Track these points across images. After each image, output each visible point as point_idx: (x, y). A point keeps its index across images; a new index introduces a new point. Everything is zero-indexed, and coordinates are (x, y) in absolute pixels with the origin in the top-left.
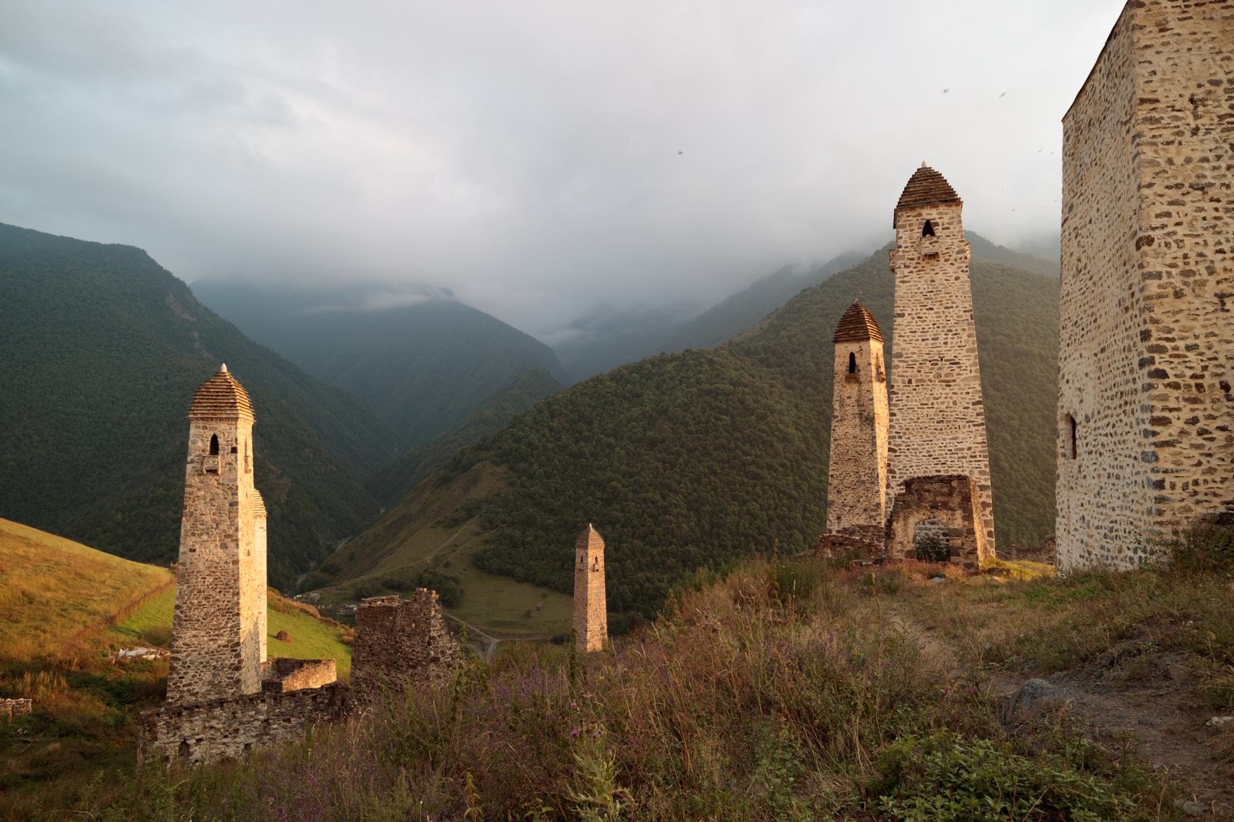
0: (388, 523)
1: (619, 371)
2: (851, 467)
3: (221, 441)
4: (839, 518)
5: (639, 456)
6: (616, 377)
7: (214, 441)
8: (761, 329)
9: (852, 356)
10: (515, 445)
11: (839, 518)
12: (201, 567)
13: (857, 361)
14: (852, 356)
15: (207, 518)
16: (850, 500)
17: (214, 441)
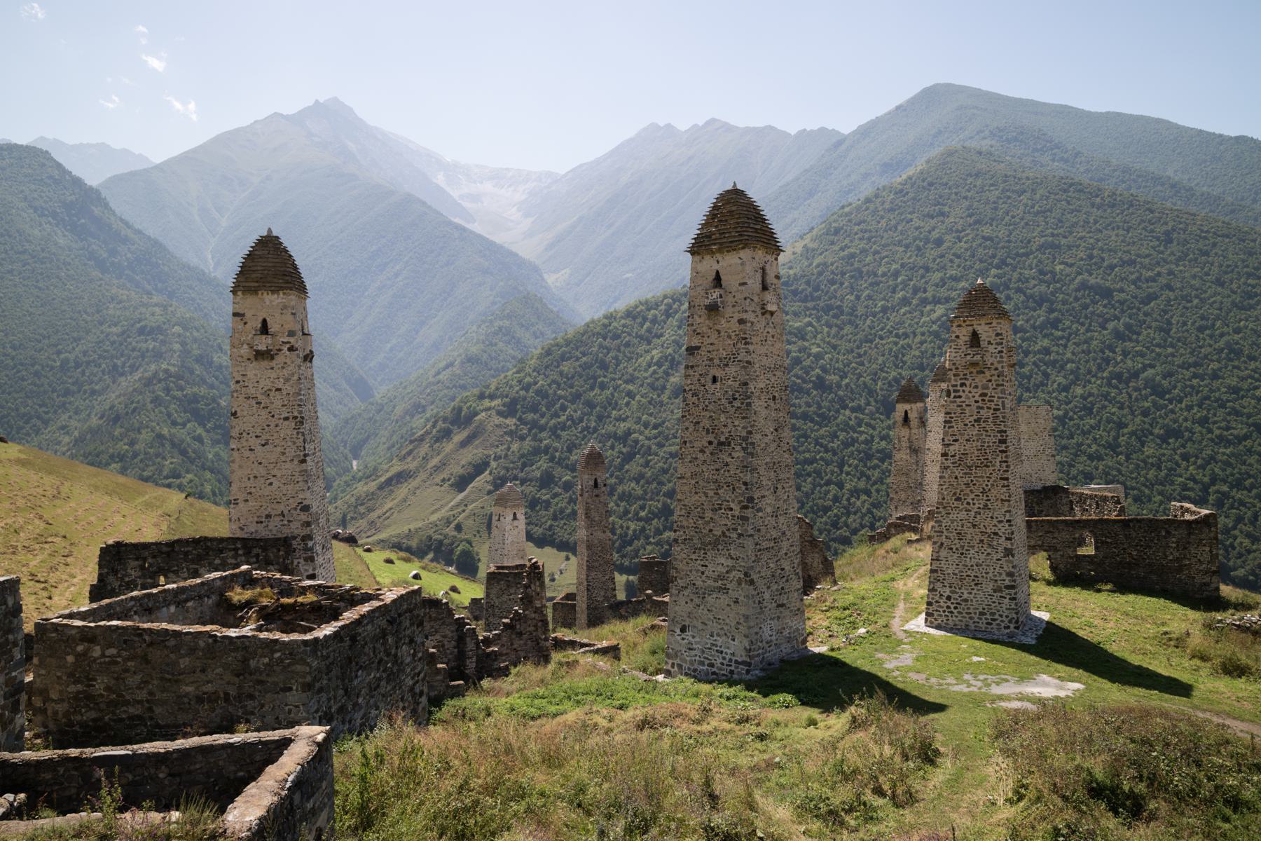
0: (383, 479)
1: (636, 307)
2: (904, 478)
3: (599, 481)
4: (896, 507)
5: (661, 406)
6: (630, 314)
7: (596, 480)
8: (794, 253)
9: (906, 412)
10: (522, 393)
11: (896, 507)
12: (596, 542)
13: (909, 415)
14: (906, 412)
15: (597, 519)
16: (903, 497)
17: (596, 480)
